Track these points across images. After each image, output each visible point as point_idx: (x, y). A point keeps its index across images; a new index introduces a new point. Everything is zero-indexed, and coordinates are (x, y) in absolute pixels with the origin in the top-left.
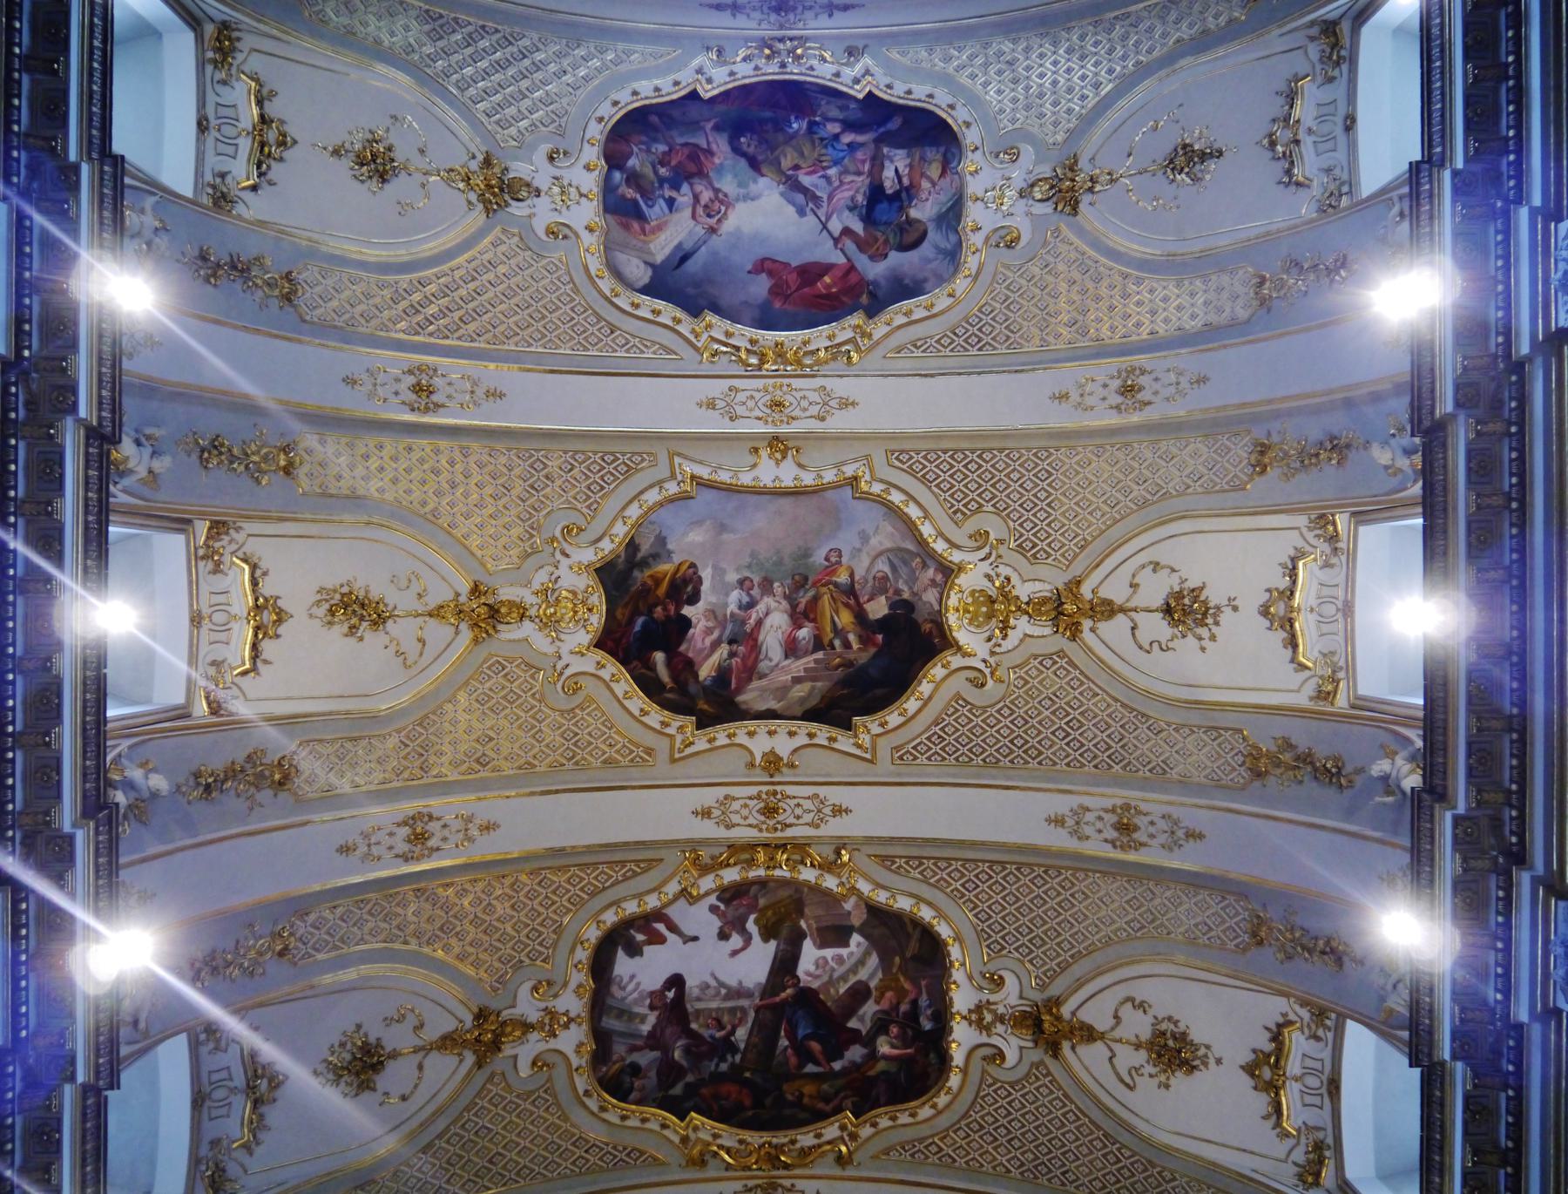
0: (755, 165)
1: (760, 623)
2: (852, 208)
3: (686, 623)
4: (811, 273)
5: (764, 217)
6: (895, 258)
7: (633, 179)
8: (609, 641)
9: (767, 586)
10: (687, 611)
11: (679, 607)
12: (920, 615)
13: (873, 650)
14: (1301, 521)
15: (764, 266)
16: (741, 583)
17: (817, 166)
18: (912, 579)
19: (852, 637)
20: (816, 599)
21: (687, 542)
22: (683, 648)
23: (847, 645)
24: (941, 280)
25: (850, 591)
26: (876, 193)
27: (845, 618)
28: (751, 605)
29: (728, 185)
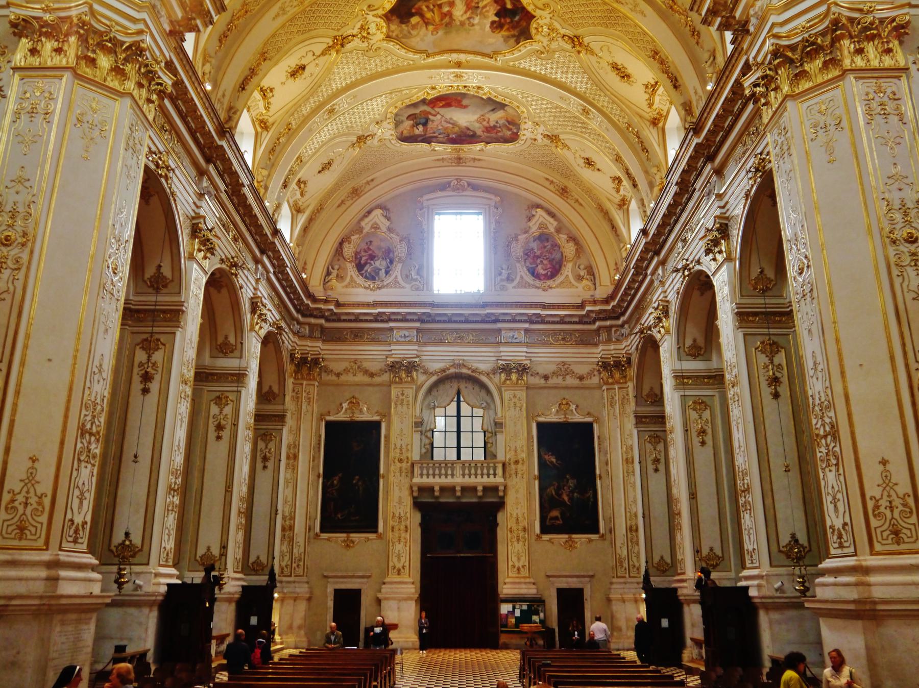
0: (468, 129)
1: (466, 12)
2: (433, 121)
3: (497, 15)
4: (448, 105)
5: (464, 118)
6: (417, 111)
7: (510, 130)
8: (529, 17)
9: (462, 24)
10: (497, 19)
11: (500, 21)
12: (397, 21)
13: (416, 6)
14: (271, 120)
15: (465, 107)
16: (473, 25)
17: (447, 128)
18: (401, 31)
19: (425, 9)
20: (442, 20)
21: (496, 40)
22: (499, 8)
23: (427, 7)
24: (401, 109)
25: (427, 24)
26: (425, 124)
27: (429, 15)
28: (469, 18)
29: (477, 125)
